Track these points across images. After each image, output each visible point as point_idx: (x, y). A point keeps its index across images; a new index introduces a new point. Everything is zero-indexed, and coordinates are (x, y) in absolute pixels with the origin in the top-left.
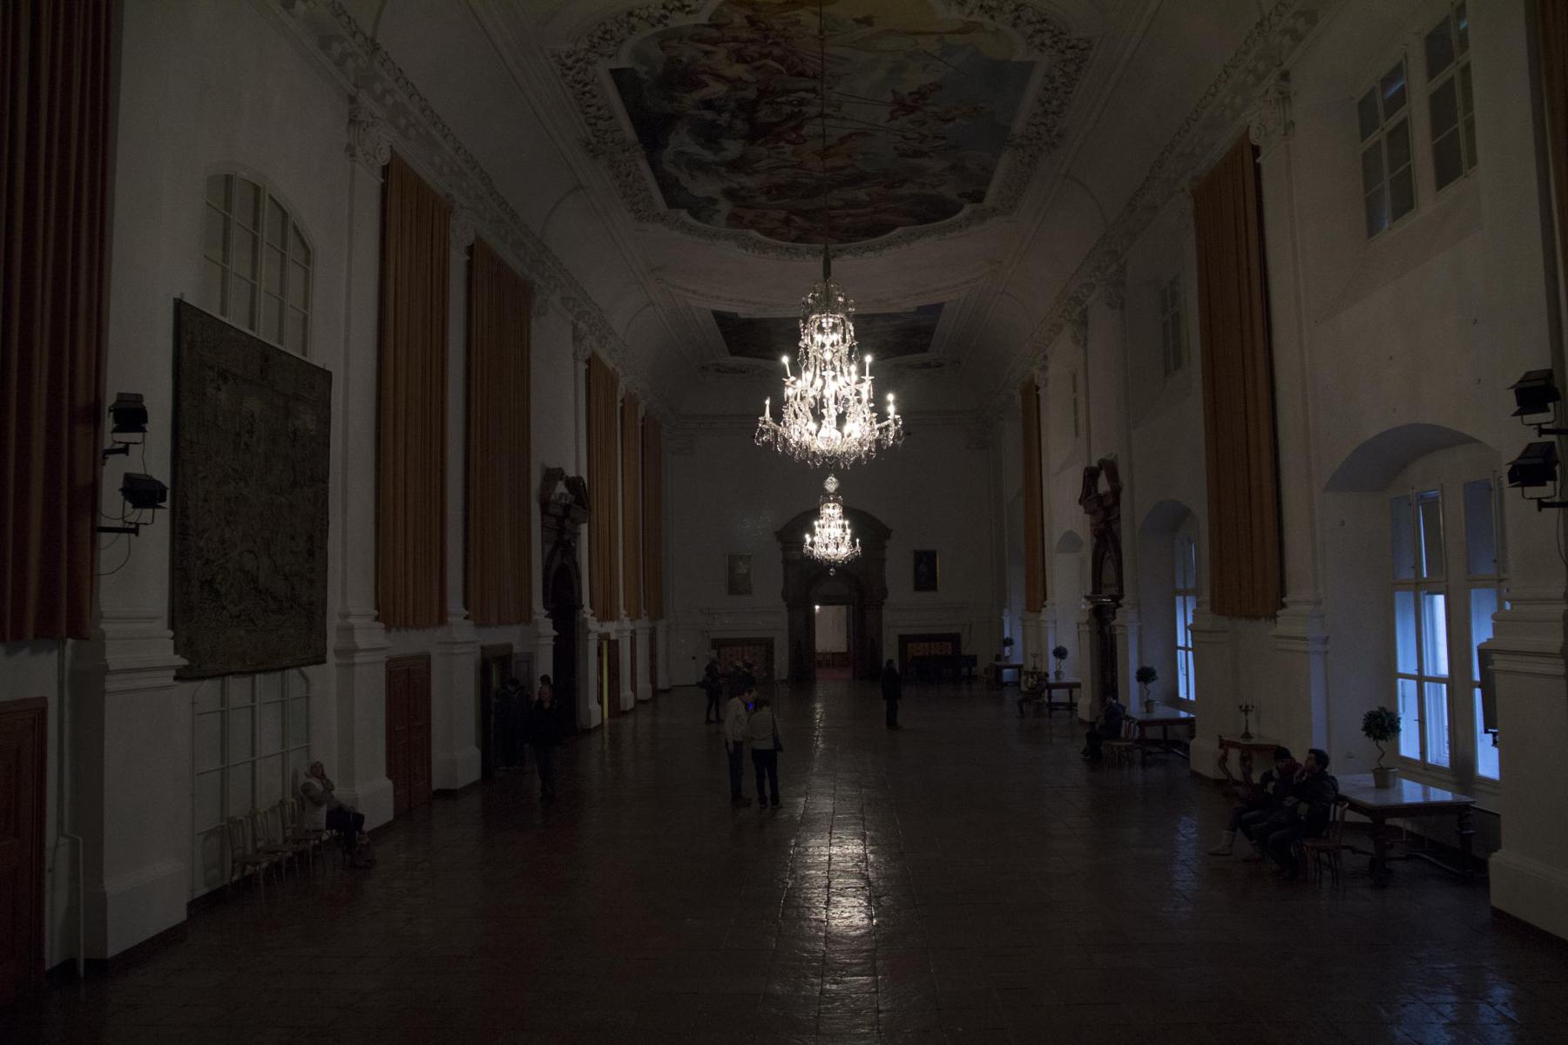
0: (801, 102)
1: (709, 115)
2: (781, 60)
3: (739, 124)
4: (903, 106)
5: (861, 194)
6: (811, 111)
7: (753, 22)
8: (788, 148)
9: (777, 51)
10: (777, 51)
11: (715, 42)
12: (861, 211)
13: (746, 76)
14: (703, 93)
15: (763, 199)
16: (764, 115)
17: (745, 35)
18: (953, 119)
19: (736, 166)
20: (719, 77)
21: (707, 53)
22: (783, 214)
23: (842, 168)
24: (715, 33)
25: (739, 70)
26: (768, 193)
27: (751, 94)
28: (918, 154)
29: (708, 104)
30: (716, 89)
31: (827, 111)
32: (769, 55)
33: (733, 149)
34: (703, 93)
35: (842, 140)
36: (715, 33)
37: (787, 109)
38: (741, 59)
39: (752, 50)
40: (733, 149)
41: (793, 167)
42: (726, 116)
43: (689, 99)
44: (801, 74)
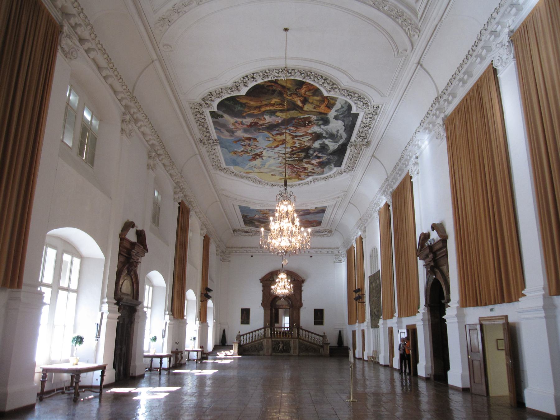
0: (290, 158)
1: (320, 155)
2: (294, 167)
3: (311, 152)
4: (259, 155)
5: (268, 119)
6: (287, 155)
7: (300, 176)
8: (297, 145)
9: (295, 169)
10: (295, 169)
11: (310, 172)
12: (268, 108)
13: (305, 164)
14: (318, 160)
15: (314, 118)
16: (303, 154)
17: (302, 173)
18: (242, 151)
19: (318, 136)
20: (312, 164)
21: (313, 169)
22: (306, 108)
23: (277, 134)
24: (309, 174)
25: (306, 166)
26: (310, 122)
27: (305, 160)
28: (249, 139)
29: (319, 158)
30: (314, 162)
31: (283, 155)
32: (297, 168)
33: (317, 145)
34: (318, 160)
35: (277, 146)
36: (309, 174)
37: (295, 156)
38: (305, 169)
39: (301, 170)
40: (317, 145)
41: (296, 137)
42: (315, 155)
43: (324, 158)
44: (289, 164)
